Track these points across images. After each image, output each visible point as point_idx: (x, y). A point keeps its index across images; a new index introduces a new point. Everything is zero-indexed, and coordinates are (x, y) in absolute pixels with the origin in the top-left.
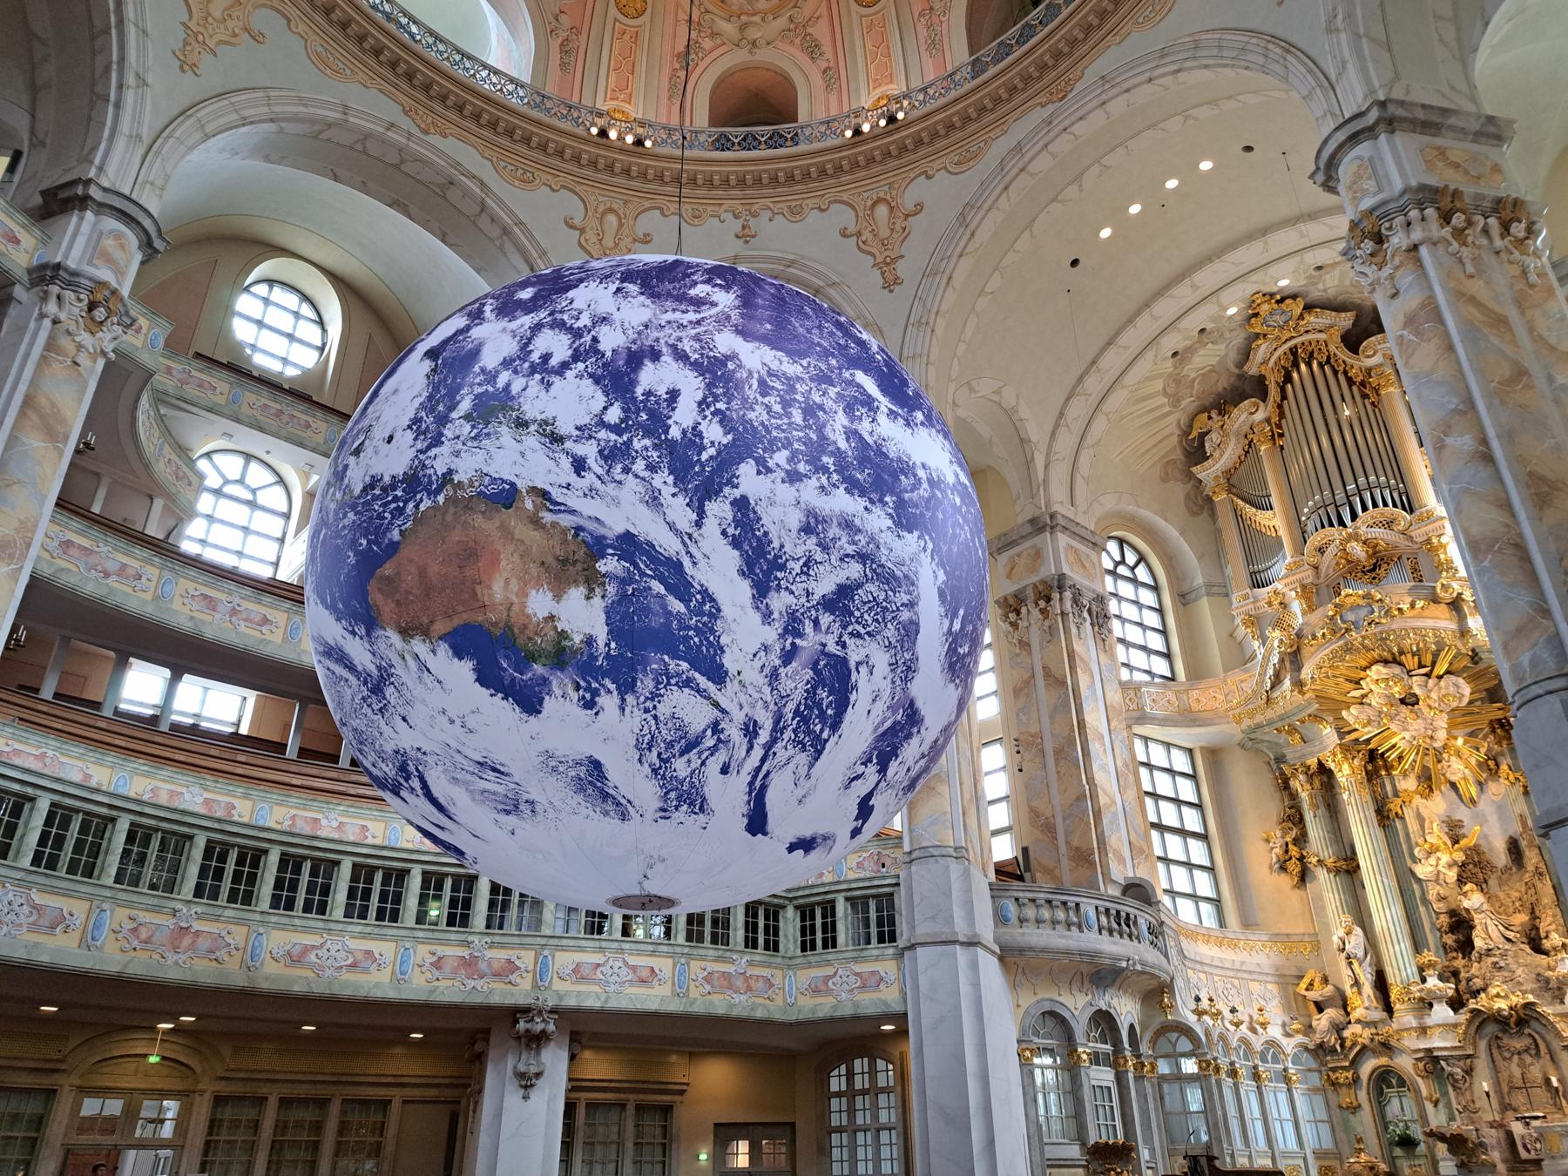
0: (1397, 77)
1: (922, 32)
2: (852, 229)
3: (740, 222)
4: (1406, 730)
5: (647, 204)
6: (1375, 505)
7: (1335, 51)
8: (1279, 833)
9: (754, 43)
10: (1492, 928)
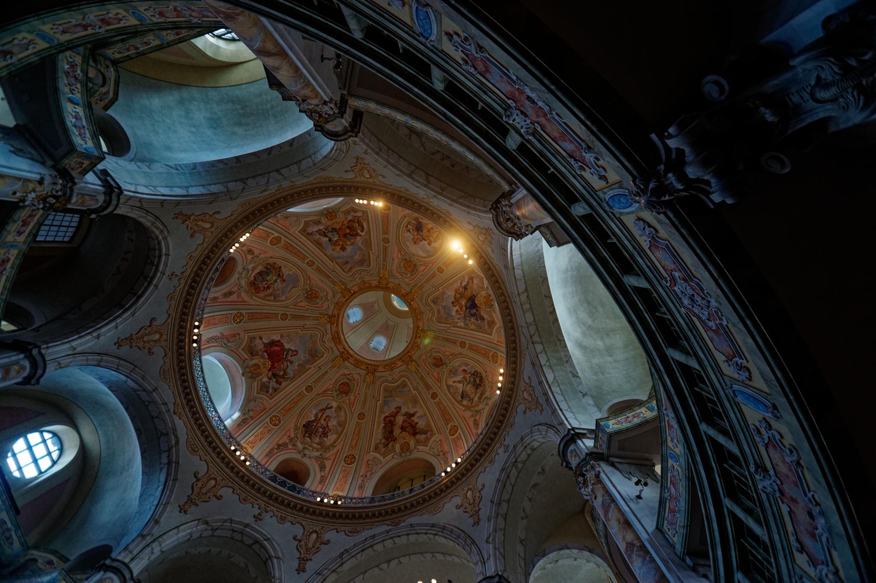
0: (505, 570)
1: (360, 481)
2: (299, 537)
3: (259, 511)
5: (230, 485)
7: (488, 549)
9: (305, 455)
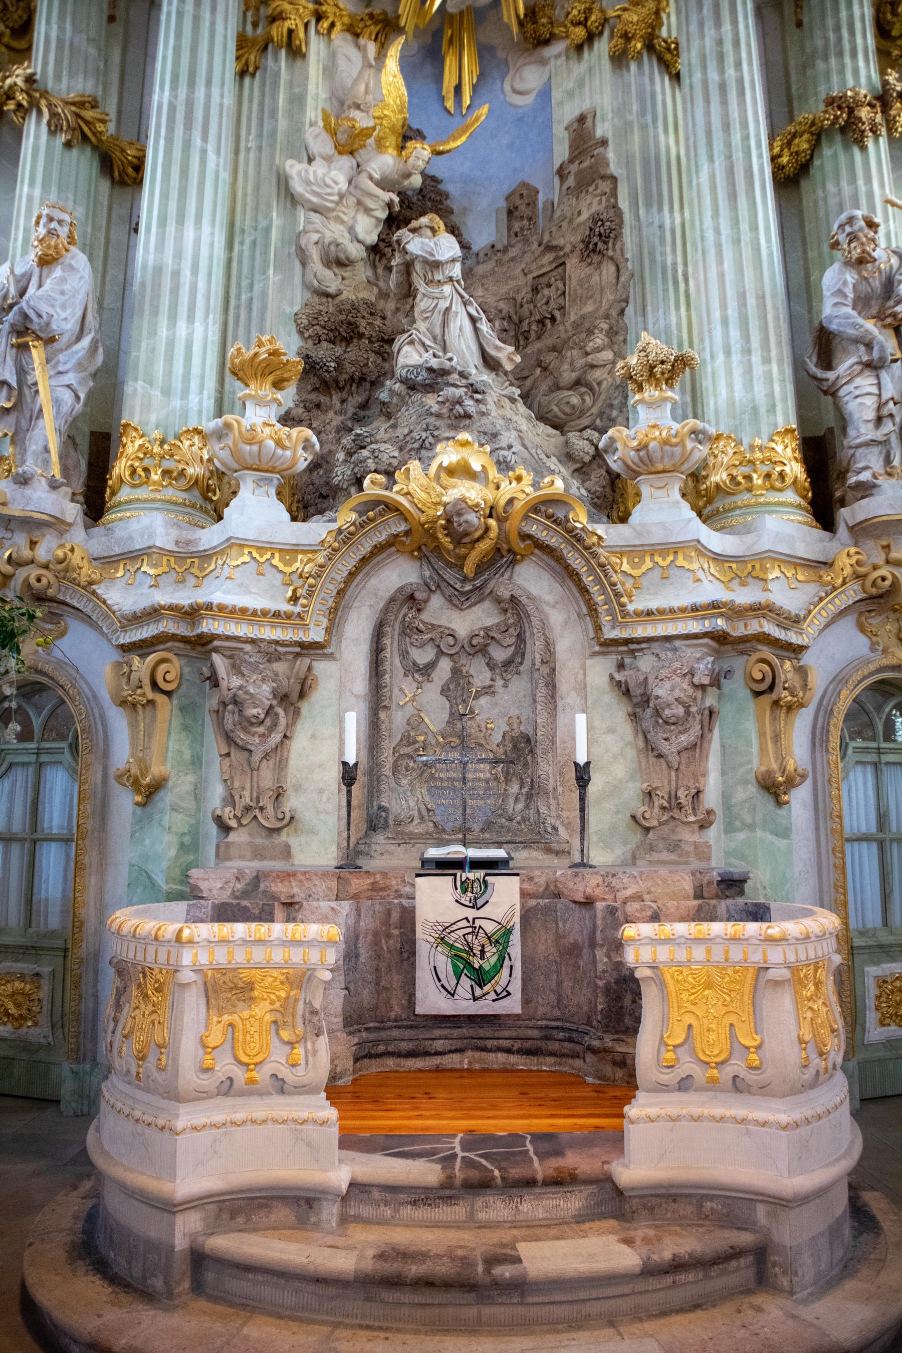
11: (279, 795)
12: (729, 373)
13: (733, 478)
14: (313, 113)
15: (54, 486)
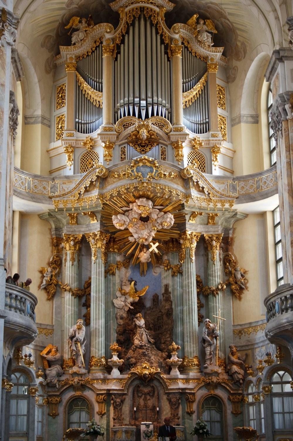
4: (136, 233)
6: (157, 114)
8: (49, 269)
10: (144, 336)
11: (121, 415)
12: (187, 345)
13: (187, 364)
14: (117, 287)
15: (84, 367)
